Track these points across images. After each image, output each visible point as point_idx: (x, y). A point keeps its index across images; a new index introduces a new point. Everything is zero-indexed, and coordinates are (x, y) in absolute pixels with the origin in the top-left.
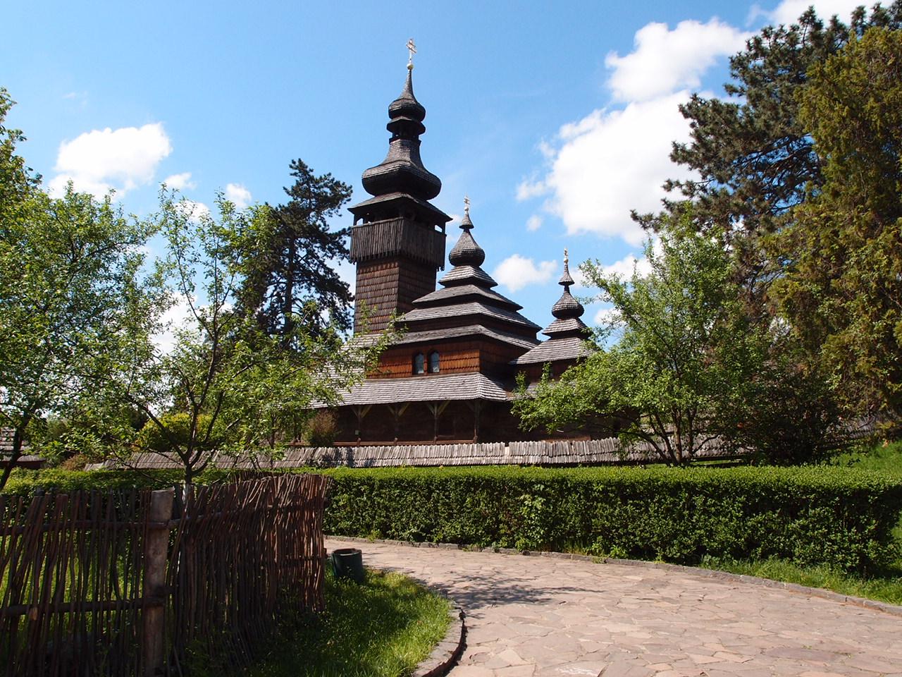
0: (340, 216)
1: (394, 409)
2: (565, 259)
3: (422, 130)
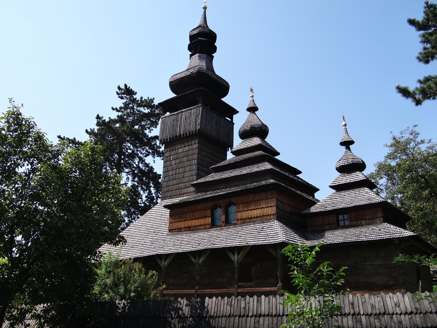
1: (195, 258)
2: (344, 123)
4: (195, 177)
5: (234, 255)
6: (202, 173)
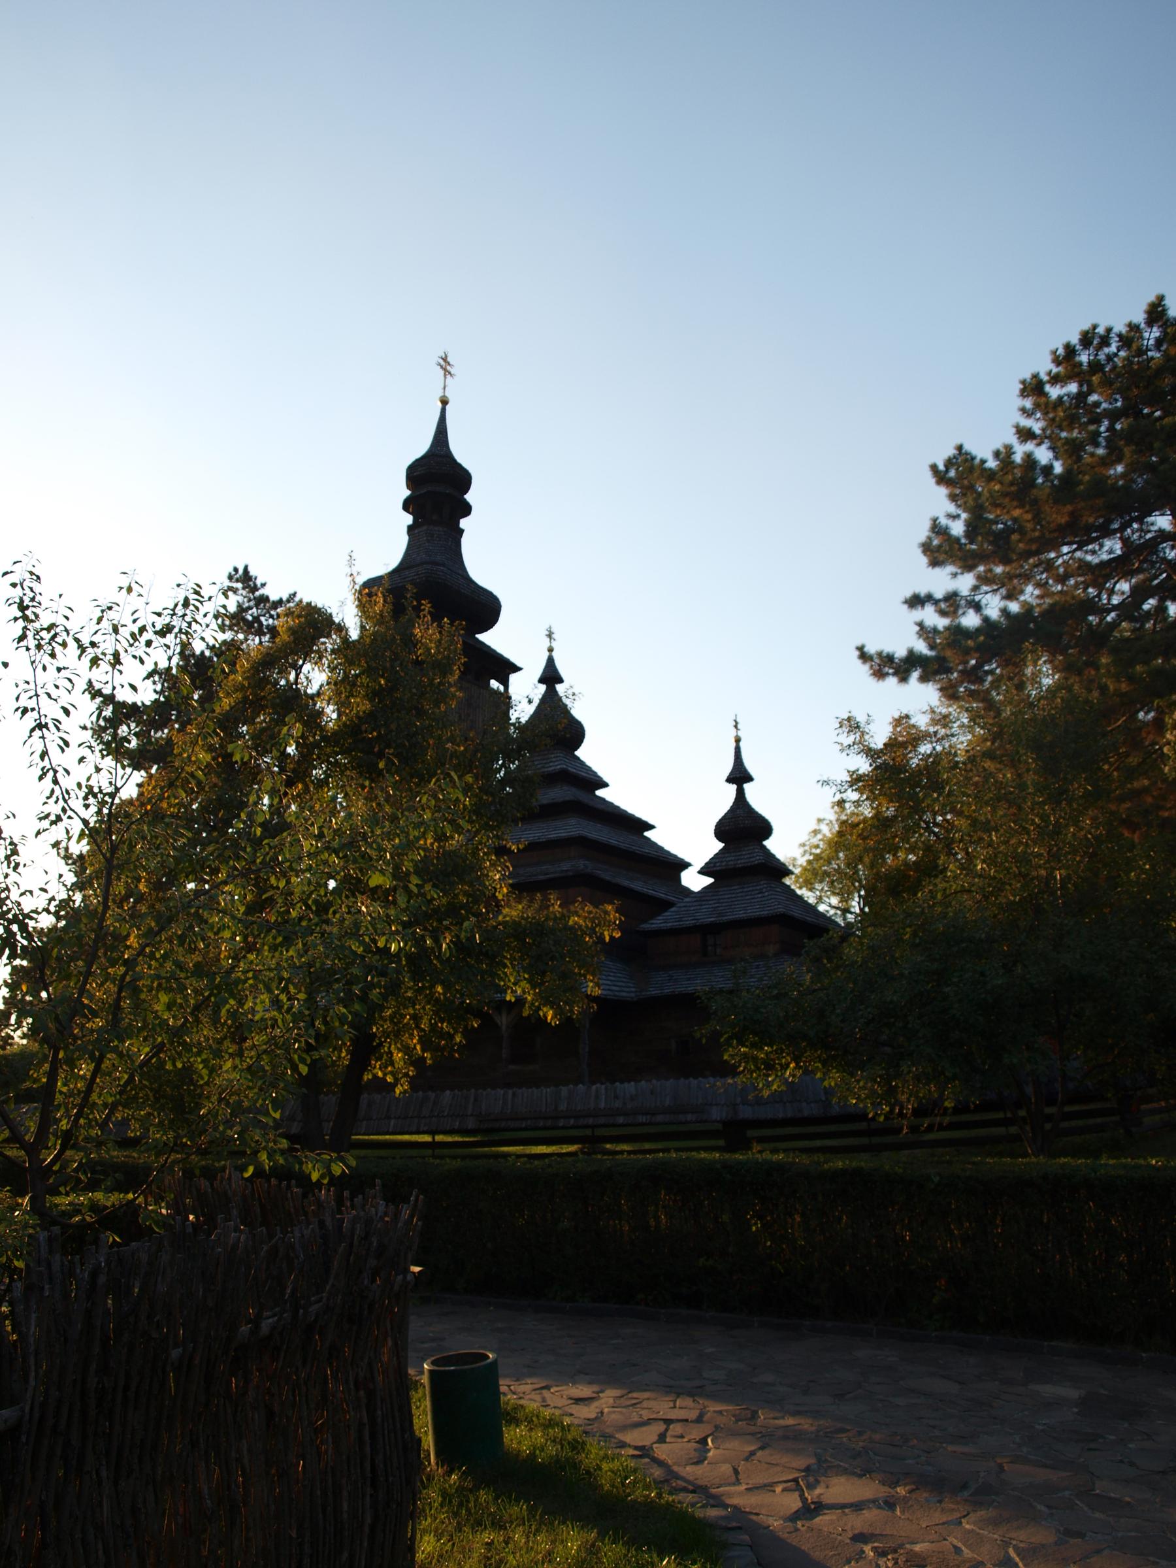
3: (466, 510)
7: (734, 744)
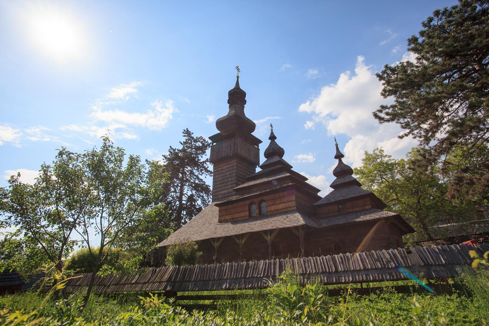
0: (206, 155)
1: (239, 240)
4: (235, 185)
5: (267, 236)
6: (240, 183)
7: (336, 146)
